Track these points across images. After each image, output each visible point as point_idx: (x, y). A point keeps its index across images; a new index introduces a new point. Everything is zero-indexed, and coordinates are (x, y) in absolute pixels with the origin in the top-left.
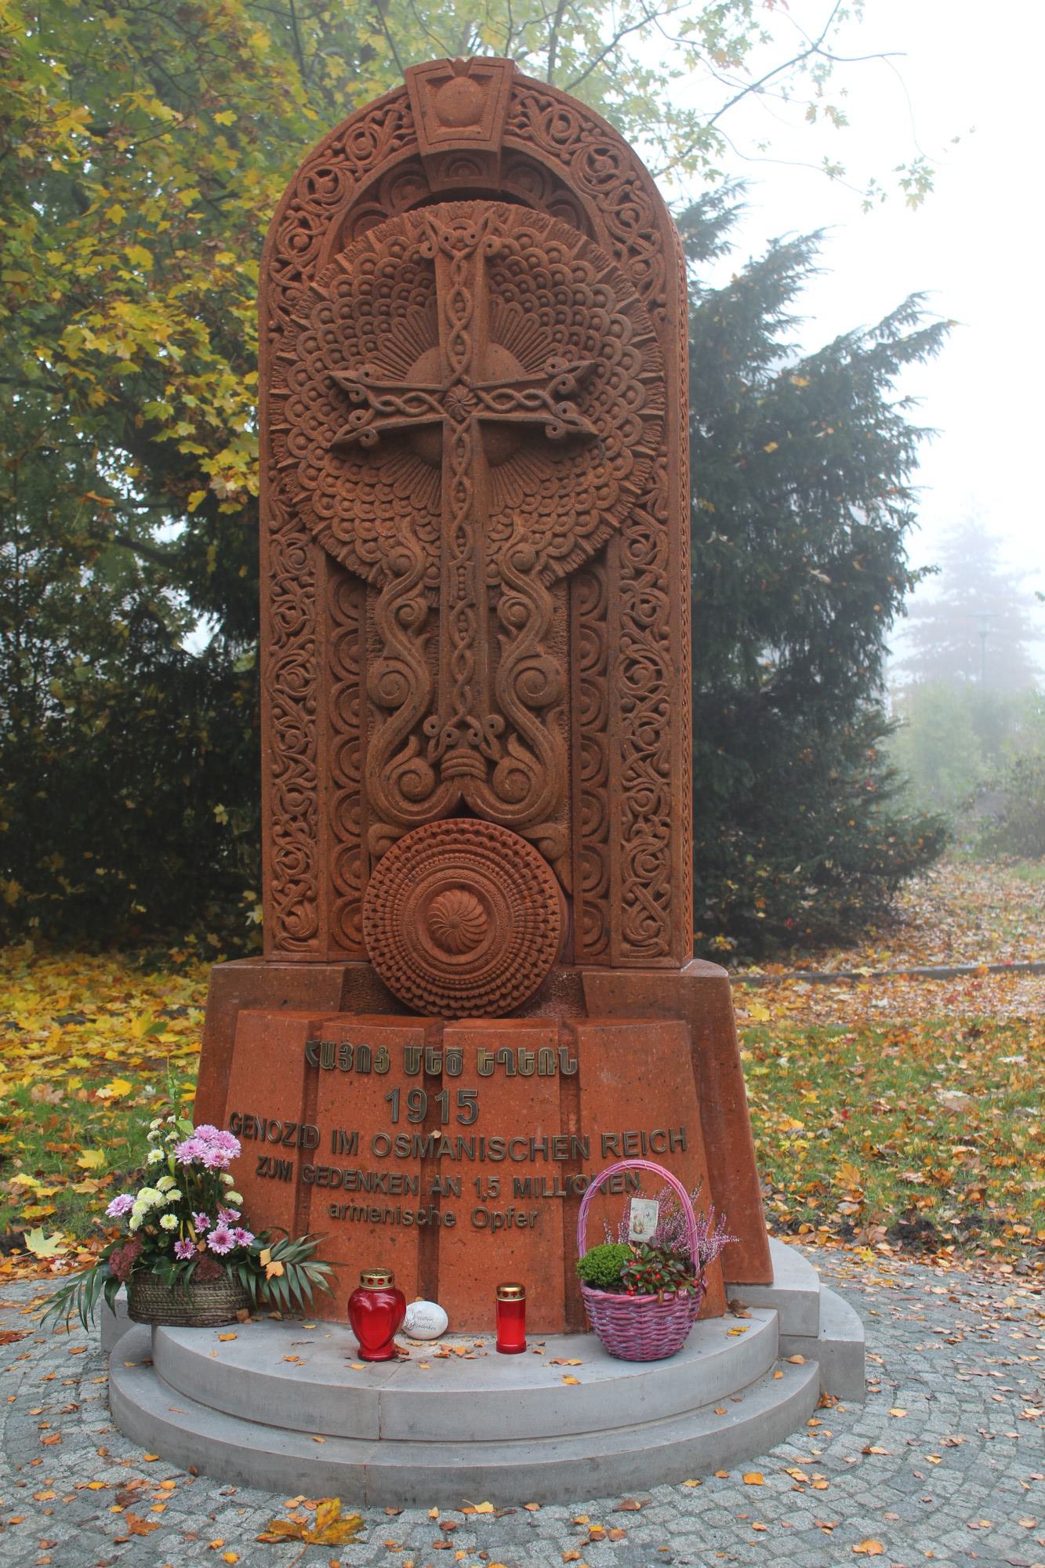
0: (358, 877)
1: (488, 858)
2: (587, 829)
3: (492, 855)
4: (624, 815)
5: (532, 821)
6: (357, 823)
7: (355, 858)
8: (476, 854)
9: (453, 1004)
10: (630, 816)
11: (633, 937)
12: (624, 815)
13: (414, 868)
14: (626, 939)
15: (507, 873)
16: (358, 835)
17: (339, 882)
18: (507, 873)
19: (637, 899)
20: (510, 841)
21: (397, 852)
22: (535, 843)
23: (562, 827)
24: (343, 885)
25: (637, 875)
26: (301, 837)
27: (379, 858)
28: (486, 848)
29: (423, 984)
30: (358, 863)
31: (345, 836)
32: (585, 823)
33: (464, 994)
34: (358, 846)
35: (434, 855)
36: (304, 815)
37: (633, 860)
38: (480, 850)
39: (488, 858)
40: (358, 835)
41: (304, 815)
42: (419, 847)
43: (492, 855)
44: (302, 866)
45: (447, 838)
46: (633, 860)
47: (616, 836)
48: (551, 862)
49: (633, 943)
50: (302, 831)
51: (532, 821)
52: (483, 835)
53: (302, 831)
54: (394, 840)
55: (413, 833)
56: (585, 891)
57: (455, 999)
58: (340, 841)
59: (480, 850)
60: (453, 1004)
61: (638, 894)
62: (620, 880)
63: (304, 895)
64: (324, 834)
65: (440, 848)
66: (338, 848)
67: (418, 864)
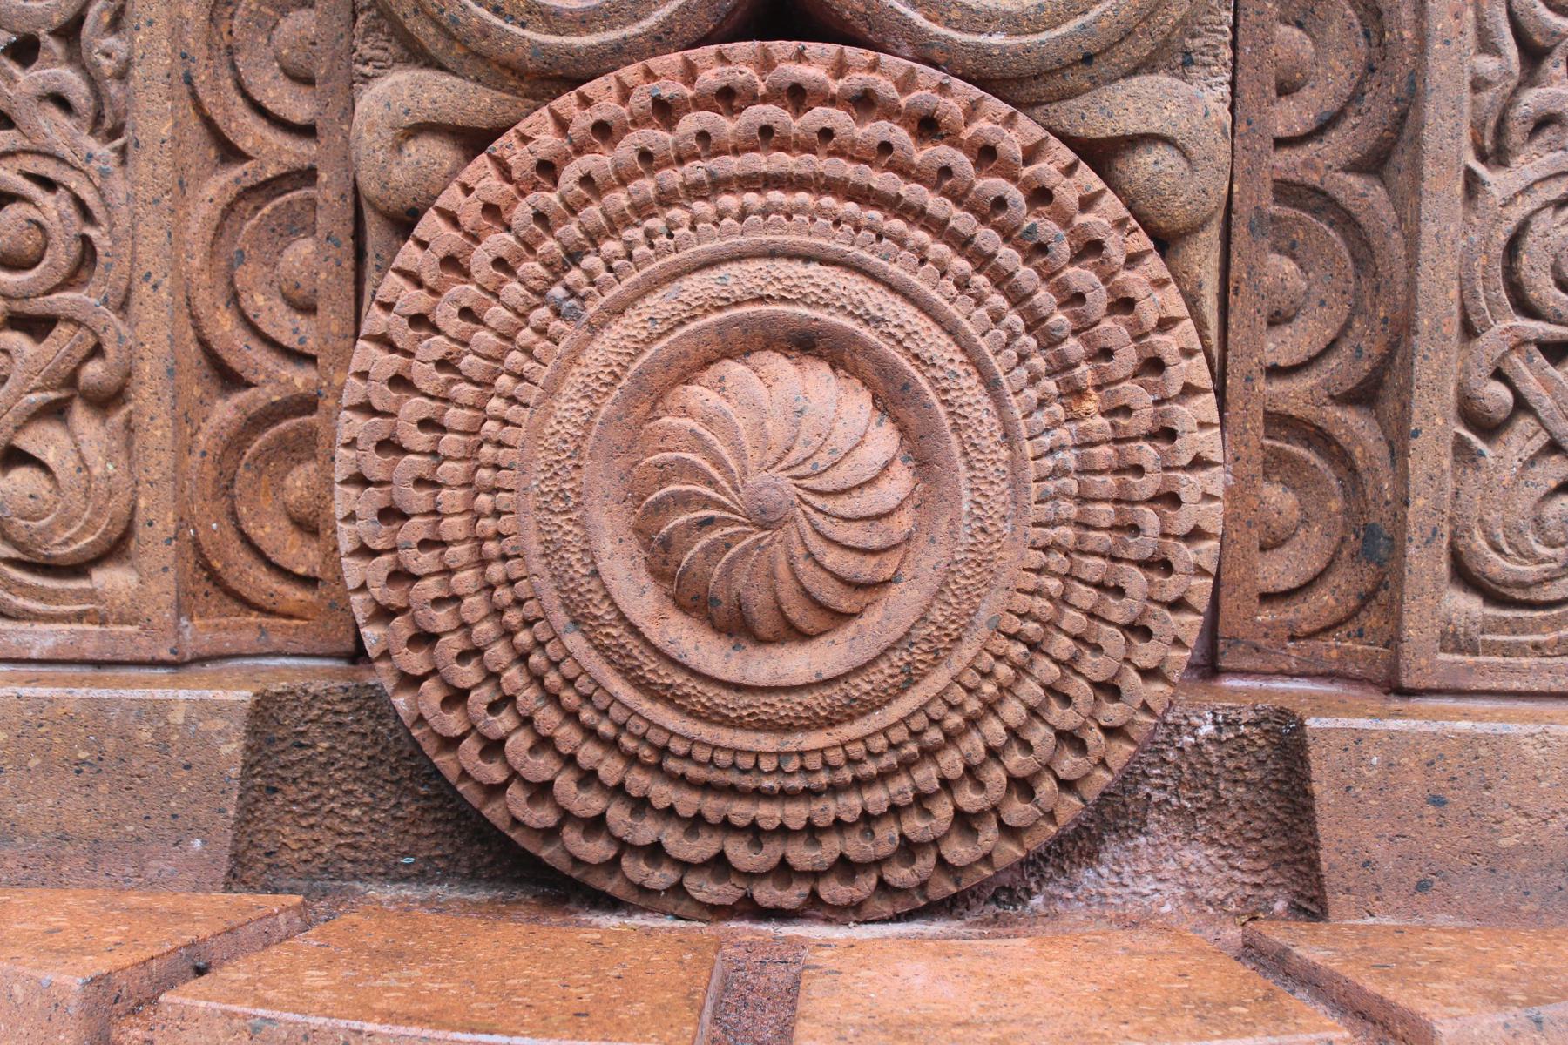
0: (307, 308)
1: (917, 215)
2: (1291, 116)
3: (935, 203)
4: (1486, 44)
5: (1090, 63)
6: (302, 78)
7: (296, 225)
8: (864, 196)
9: (740, 853)
10: (1512, 51)
11: (1498, 566)
12: (1486, 44)
13: (573, 256)
14: (1464, 575)
15: (1002, 280)
16: (306, 131)
17: (225, 329)
18: (1002, 280)
19: (1522, 405)
20: (1012, 143)
21: (489, 184)
22: (1101, 154)
23: (1212, 95)
24: (241, 338)
25: (1527, 309)
26: (53, 127)
27: (404, 223)
28: (906, 171)
29: (611, 769)
30: (304, 248)
31: (249, 132)
32: (1286, 89)
33: (796, 814)
34: (307, 176)
35: (666, 199)
36: (70, 32)
37: (1513, 246)
38: (880, 180)
39: (917, 215)
40: (306, 131)
41: (70, 32)
42: (599, 162)
43: (935, 203)
44: (61, 255)
45: (727, 126)
46: (1513, 246)
47: (1447, 134)
48: (1166, 242)
49: (1493, 594)
50: (61, 101)
51: (1090, 63)
52: (891, 112)
53: (61, 101)
54: (473, 140)
55: (567, 102)
56: (1274, 372)
57: (755, 833)
58: (230, 153)
59: (880, 180)
60: (740, 853)
61: (1531, 386)
62: (1453, 328)
63: (71, 380)
64: (156, 118)
65: (695, 170)
66: (221, 183)
67: (594, 237)
